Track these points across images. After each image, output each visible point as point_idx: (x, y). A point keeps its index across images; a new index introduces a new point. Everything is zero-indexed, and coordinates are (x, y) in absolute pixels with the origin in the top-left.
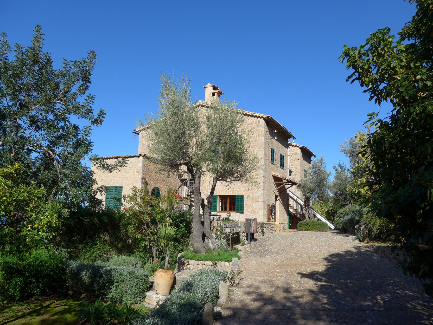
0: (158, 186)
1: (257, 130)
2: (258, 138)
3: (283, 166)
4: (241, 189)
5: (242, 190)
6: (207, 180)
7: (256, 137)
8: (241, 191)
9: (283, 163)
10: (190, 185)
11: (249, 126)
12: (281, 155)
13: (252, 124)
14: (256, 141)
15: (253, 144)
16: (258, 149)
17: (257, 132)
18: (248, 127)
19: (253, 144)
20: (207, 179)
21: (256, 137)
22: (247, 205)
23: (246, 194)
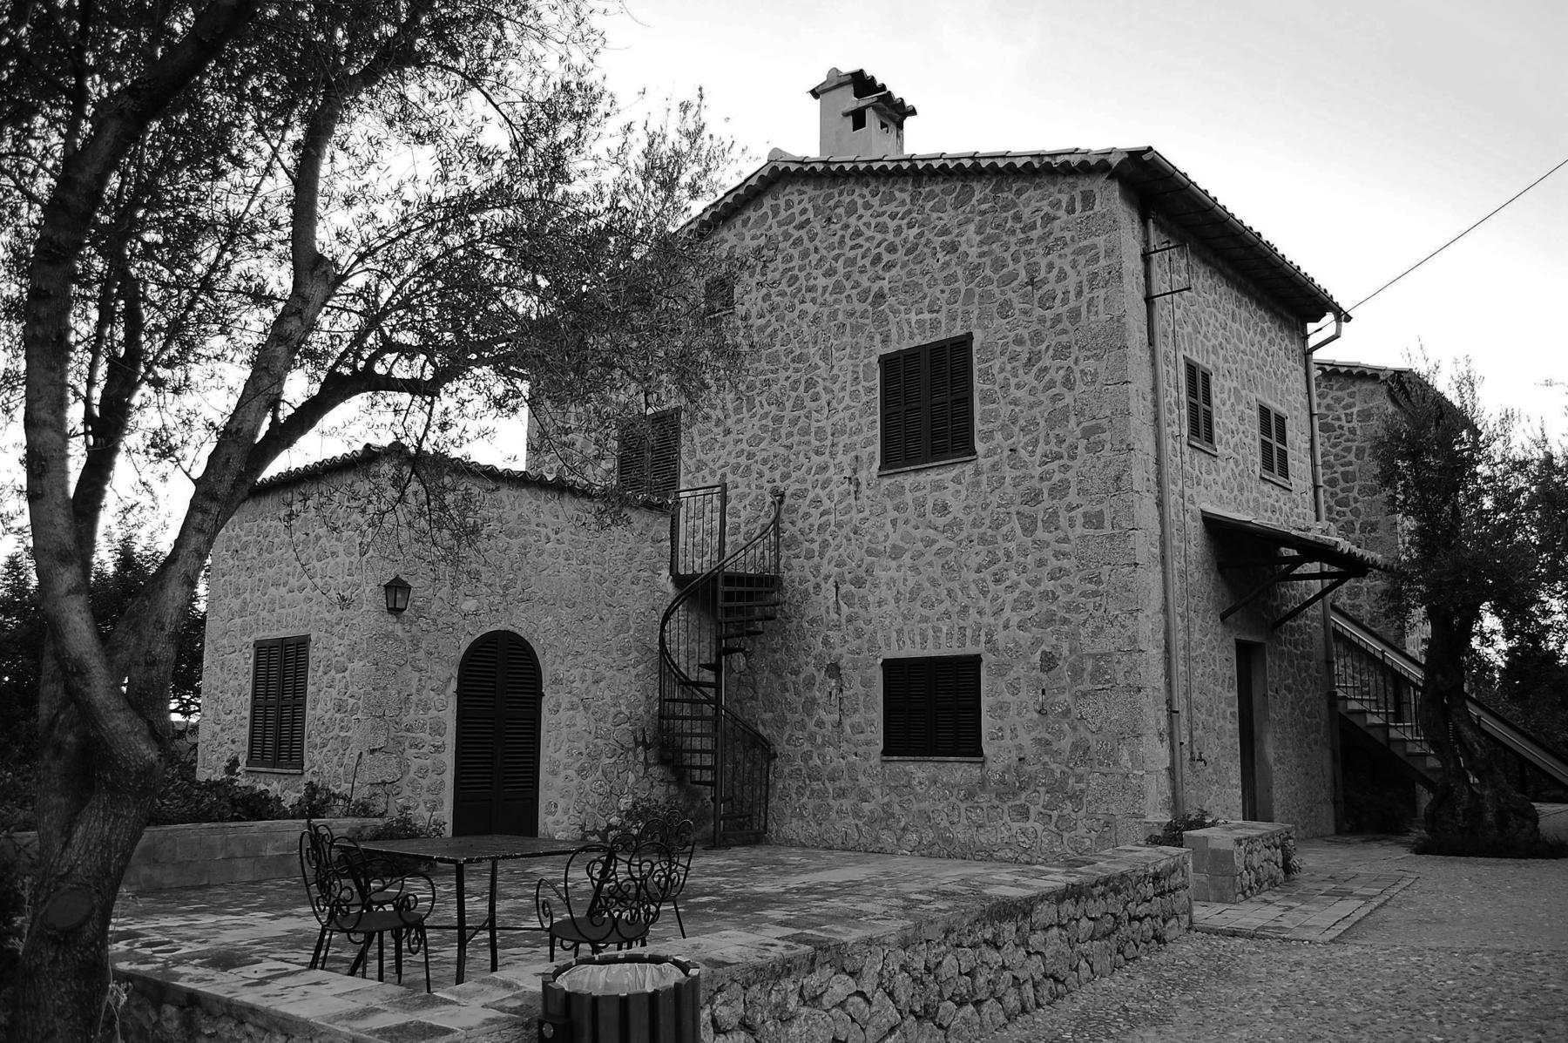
0: (518, 622)
1: (1080, 251)
2: (1086, 295)
3: (1210, 438)
4: (1007, 613)
5: (1015, 620)
6: (827, 578)
7: (1079, 293)
8: (1006, 627)
9: (1208, 415)
10: (728, 611)
11: (1034, 234)
12: (1191, 369)
13: (1048, 219)
14: (1075, 315)
15: (1064, 339)
16: (1090, 366)
17: (1082, 260)
18: (1029, 241)
19: (1064, 339)
20: (824, 571)
21: (1079, 293)
22: (437, 730)
23: (1037, 642)
